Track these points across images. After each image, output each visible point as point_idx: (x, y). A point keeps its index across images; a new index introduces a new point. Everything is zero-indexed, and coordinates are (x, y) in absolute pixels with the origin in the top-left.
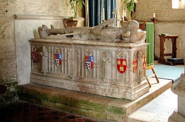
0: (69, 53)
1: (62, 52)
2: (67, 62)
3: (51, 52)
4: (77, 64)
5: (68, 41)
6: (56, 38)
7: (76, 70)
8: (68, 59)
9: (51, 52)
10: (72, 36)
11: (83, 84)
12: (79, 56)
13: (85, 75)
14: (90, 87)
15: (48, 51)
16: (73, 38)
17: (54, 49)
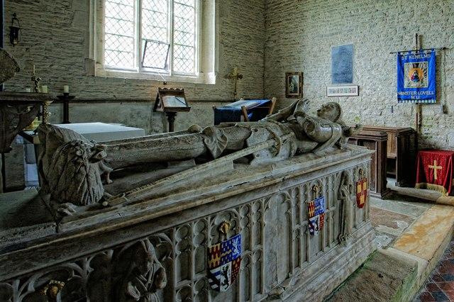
0: (265, 221)
1: (241, 225)
2: (260, 252)
3: (186, 248)
4: (285, 241)
5: (257, 177)
6: (197, 179)
7: (284, 260)
8: (260, 241)
9: (186, 248)
10: (250, 158)
11: (310, 286)
12: (293, 211)
13: (306, 260)
14: (324, 282)
15: (165, 252)
16: (253, 163)
17: (203, 230)
